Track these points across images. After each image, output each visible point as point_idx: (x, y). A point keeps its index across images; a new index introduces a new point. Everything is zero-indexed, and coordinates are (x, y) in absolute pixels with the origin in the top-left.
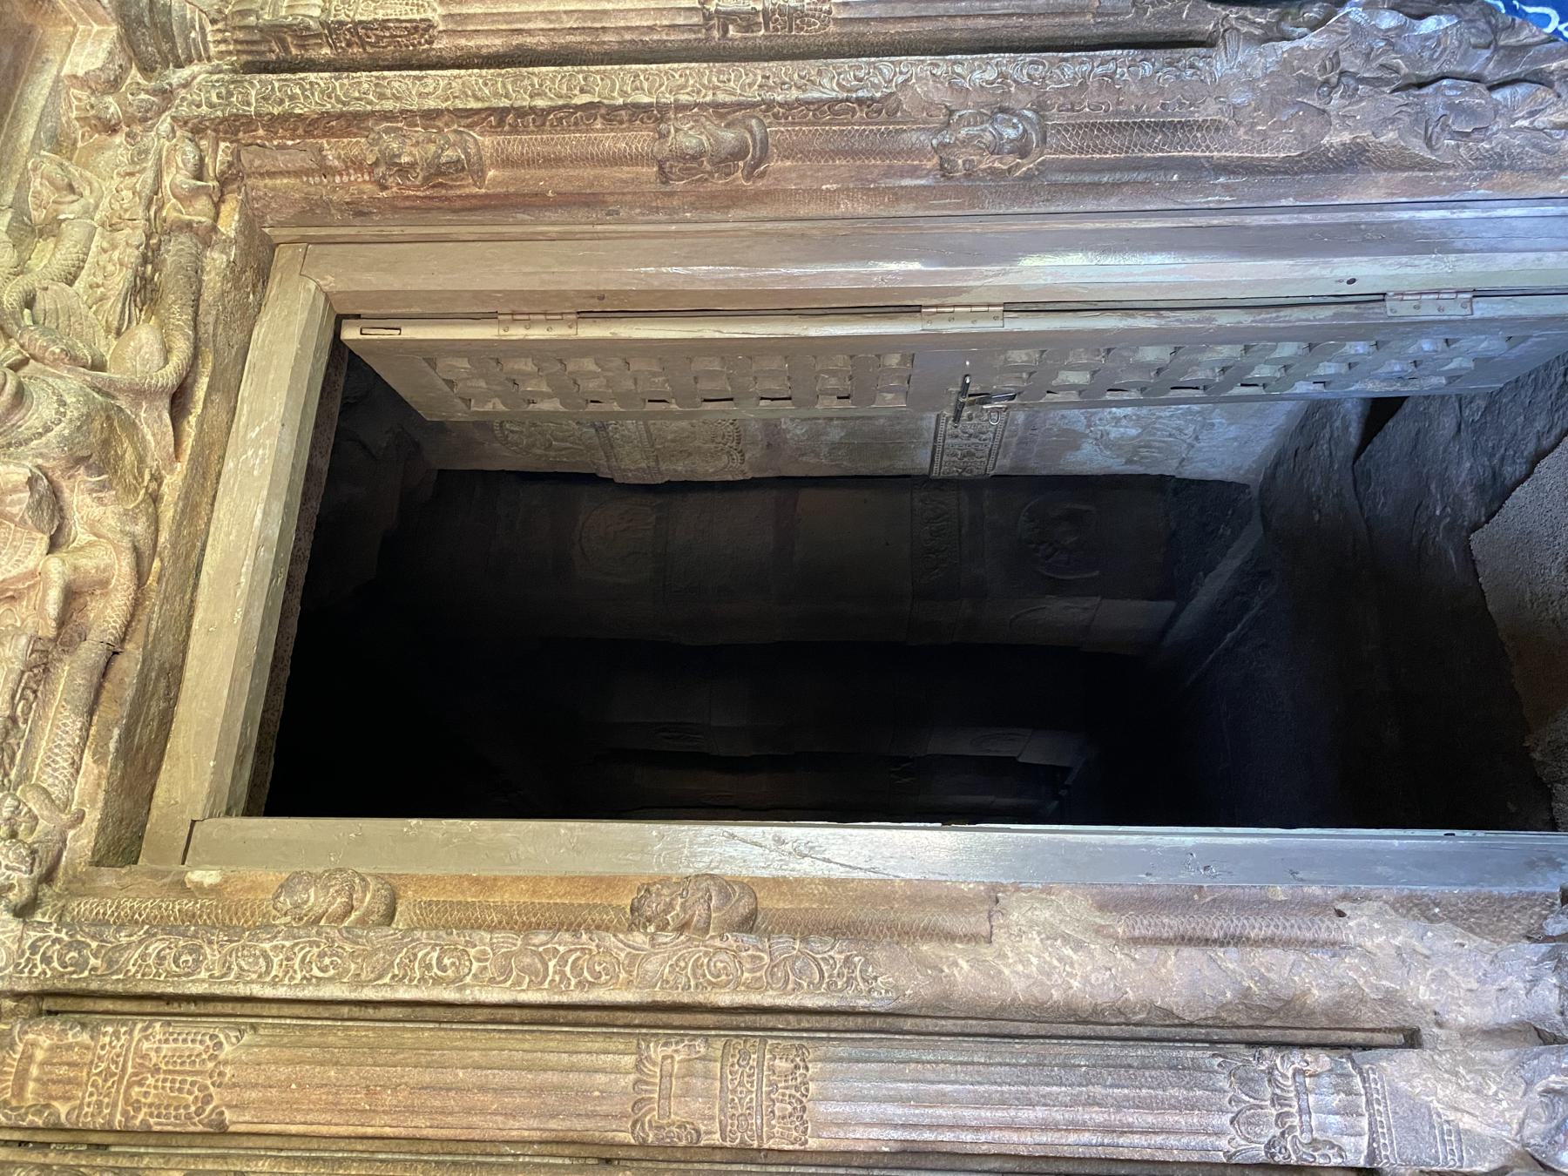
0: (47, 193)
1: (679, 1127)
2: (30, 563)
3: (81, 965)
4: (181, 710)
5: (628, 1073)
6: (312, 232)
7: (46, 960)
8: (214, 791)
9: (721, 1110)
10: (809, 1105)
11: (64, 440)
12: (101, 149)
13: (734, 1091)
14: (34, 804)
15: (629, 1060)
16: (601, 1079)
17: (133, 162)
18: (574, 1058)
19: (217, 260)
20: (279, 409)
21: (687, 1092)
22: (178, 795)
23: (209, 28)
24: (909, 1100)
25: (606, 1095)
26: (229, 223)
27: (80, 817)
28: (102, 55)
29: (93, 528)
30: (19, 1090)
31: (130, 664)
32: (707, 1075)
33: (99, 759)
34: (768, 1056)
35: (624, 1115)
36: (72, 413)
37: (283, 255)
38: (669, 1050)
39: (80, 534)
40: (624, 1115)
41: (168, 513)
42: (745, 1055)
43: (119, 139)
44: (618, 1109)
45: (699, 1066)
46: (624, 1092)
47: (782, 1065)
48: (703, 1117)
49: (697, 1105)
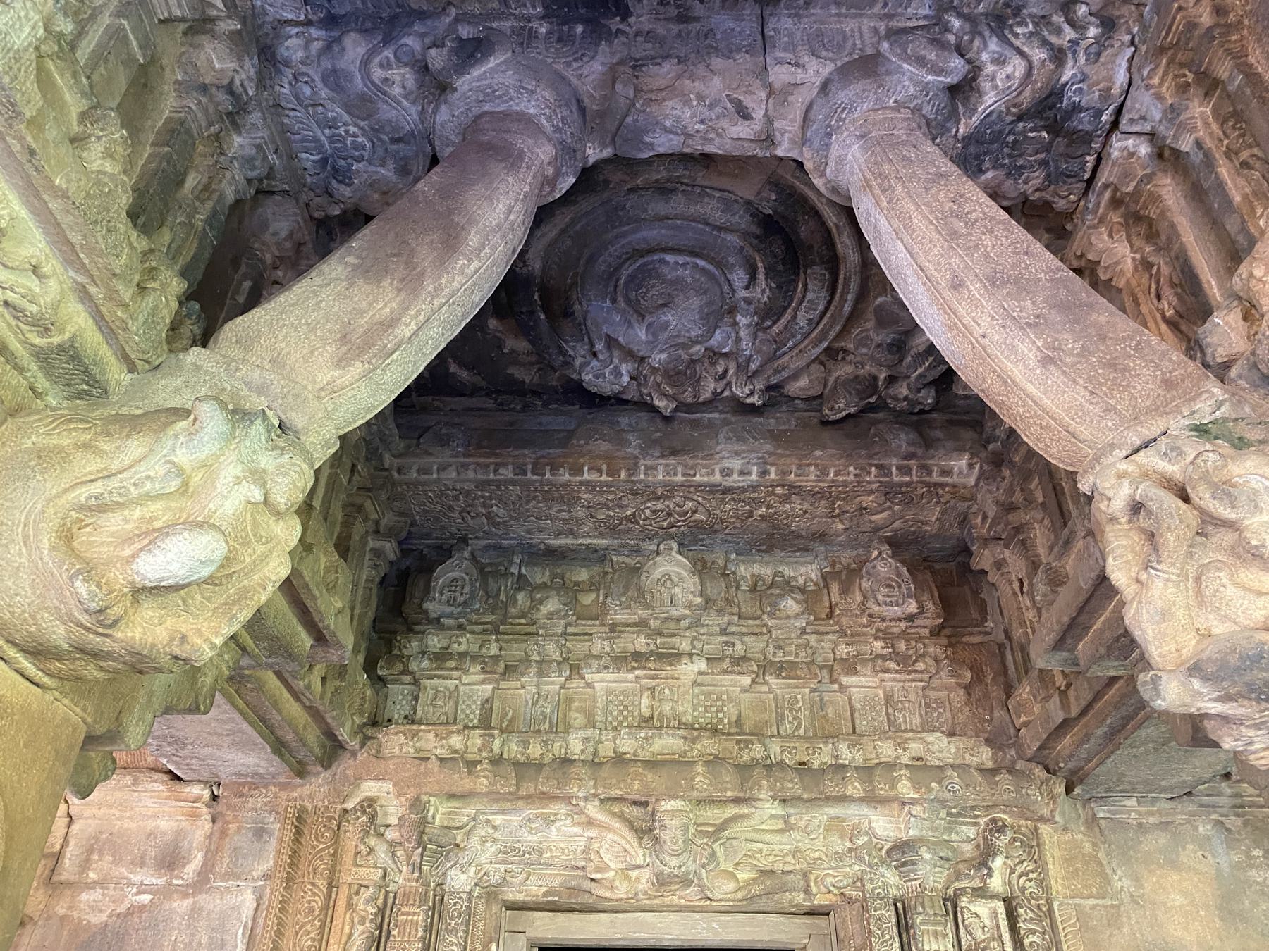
0: (802, 824)
2: (613, 865)
3: (451, 919)
4: (575, 916)
6: (834, 939)
7: (455, 904)
8: (538, 939)
11: (662, 872)
12: (842, 837)
14: (521, 877)
17: (836, 853)
19: (800, 898)
20: (729, 937)
22: (537, 923)
23: (918, 882)
26: (821, 900)
27: (520, 892)
28: (885, 834)
29: (638, 879)
30: (403, 914)
31: (586, 900)
33: (545, 894)
36: (676, 872)
37: (820, 922)
39: (634, 874)
41: (658, 901)
43: (848, 844)
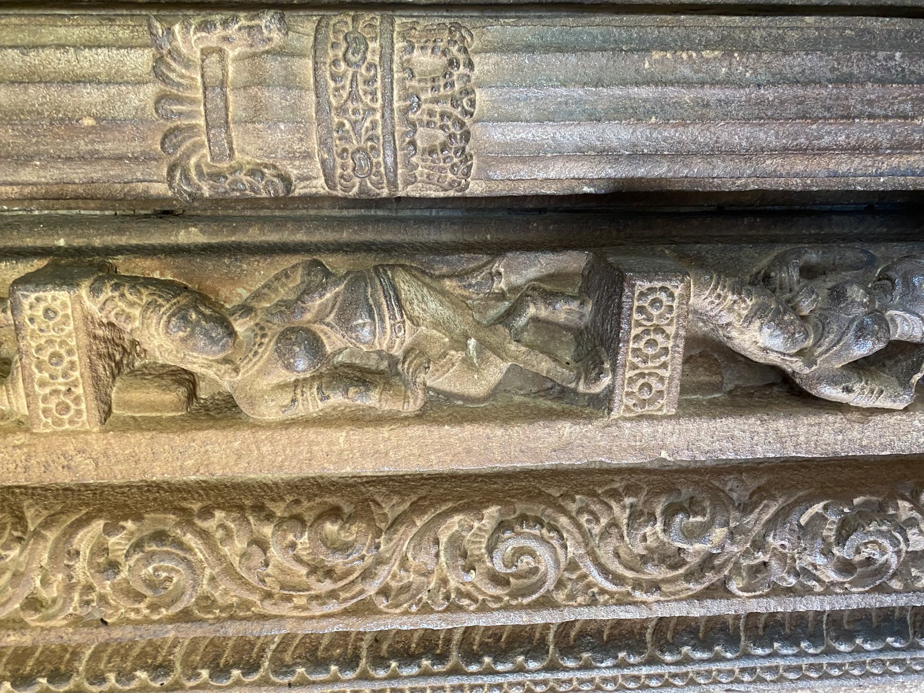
1: (252, 173)
5: (140, 83)
9: (323, 143)
10: (476, 130)
13: (342, 110)
15: (139, 60)
16: (91, 95)
18: (33, 58)
21: (257, 113)
24: (649, 114)
25: (107, 124)
32: (289, 83)
34: (399, 45)
35: (148, 158)
38: (213, 38)
40: (148, 158)
42: (356, 43)
44: (136, 147)
45: (273, 66)
46: (139, 120)
47: (424, 60)
48: (292, 156)
49: (280, 136)
